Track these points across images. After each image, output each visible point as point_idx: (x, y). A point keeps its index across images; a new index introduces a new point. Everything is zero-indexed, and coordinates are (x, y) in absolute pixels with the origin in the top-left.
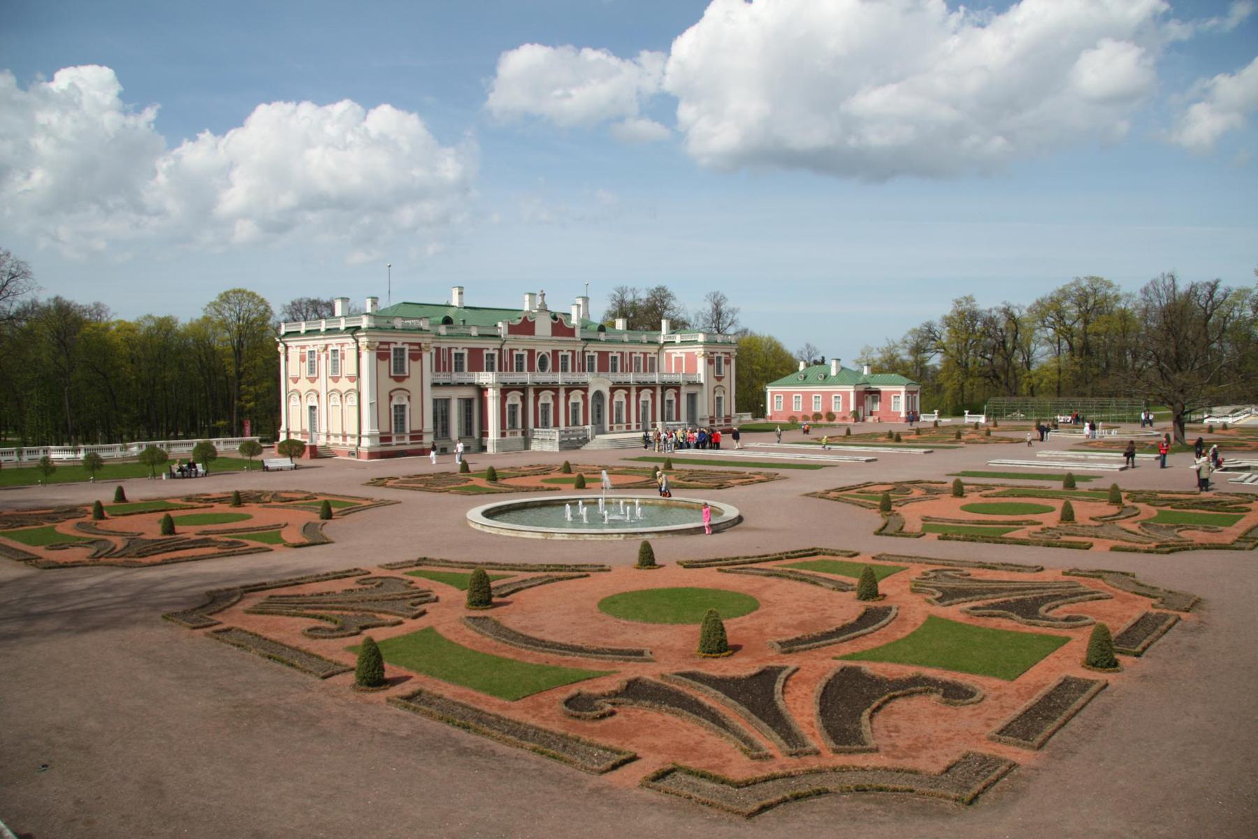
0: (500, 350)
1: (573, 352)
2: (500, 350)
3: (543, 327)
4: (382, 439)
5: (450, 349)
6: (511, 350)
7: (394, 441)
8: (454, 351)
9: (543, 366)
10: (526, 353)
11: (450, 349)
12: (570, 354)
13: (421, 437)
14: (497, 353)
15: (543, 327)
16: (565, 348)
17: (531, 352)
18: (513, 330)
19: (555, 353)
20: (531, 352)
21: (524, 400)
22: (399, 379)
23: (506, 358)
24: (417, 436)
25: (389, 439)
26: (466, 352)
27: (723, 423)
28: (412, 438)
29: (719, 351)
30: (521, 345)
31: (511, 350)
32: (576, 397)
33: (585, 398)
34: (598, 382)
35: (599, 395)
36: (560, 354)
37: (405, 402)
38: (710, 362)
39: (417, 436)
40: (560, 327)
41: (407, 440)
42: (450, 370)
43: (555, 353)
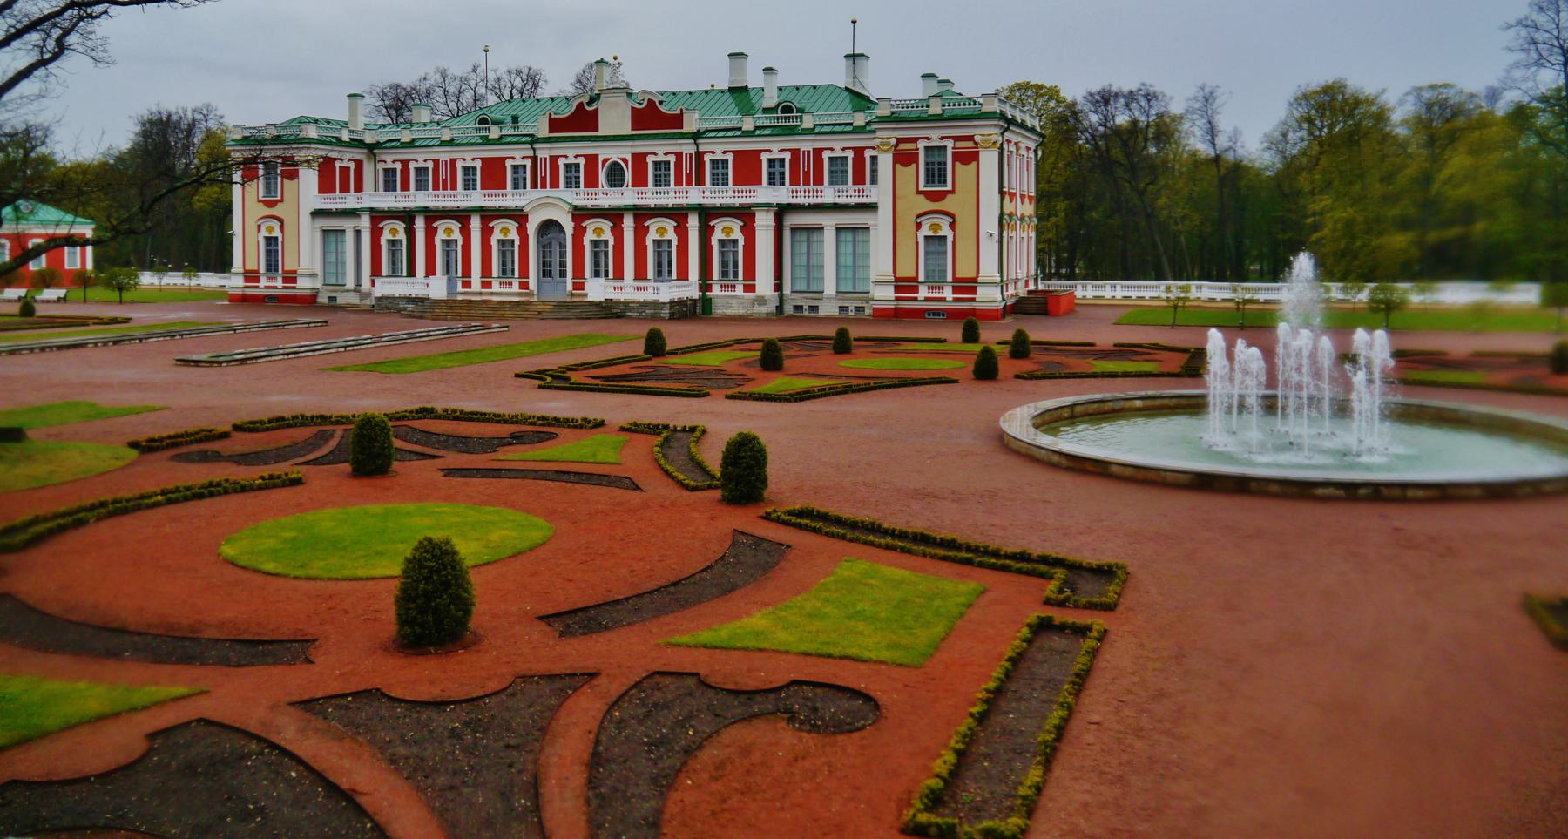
0: (534, 159)
1: (679, 155)
2: (534, 159)
3: (615, 119)
4: (247, 279)
5: (453, 161)
6: (554, 159)
7: (264, 282)
8: (459, 165)
9: (592, 182)
10: (582, 161)
11: (453, 161)
12: (672, 159)
13: (294, 280)
14: (528, 163)
15: (615, 119)
16: (659, 151)
17: (592, 160)
18: (555, 125)
19: (639, 160)
20: (592, 160)
21: (411, 233)
22: (271, 204)
23: (545, 171)
24: (291, 277)
25: (257, 280)
26: (478, 164)
27: (948, 293)
28: (285, 280)
29: (935, 135)
30: (571, 152)
31: (554, 159)
32: (504, 229)
33: (522, 231)
34: (551, 204)
35: (549, 226)
36: (650, 160)
37: (277, 233)
38: (904, 160)
39: (291, 277)
40: (652, 117)
41: (280, 279)
42: (454, 187)
43: (639, 160)
